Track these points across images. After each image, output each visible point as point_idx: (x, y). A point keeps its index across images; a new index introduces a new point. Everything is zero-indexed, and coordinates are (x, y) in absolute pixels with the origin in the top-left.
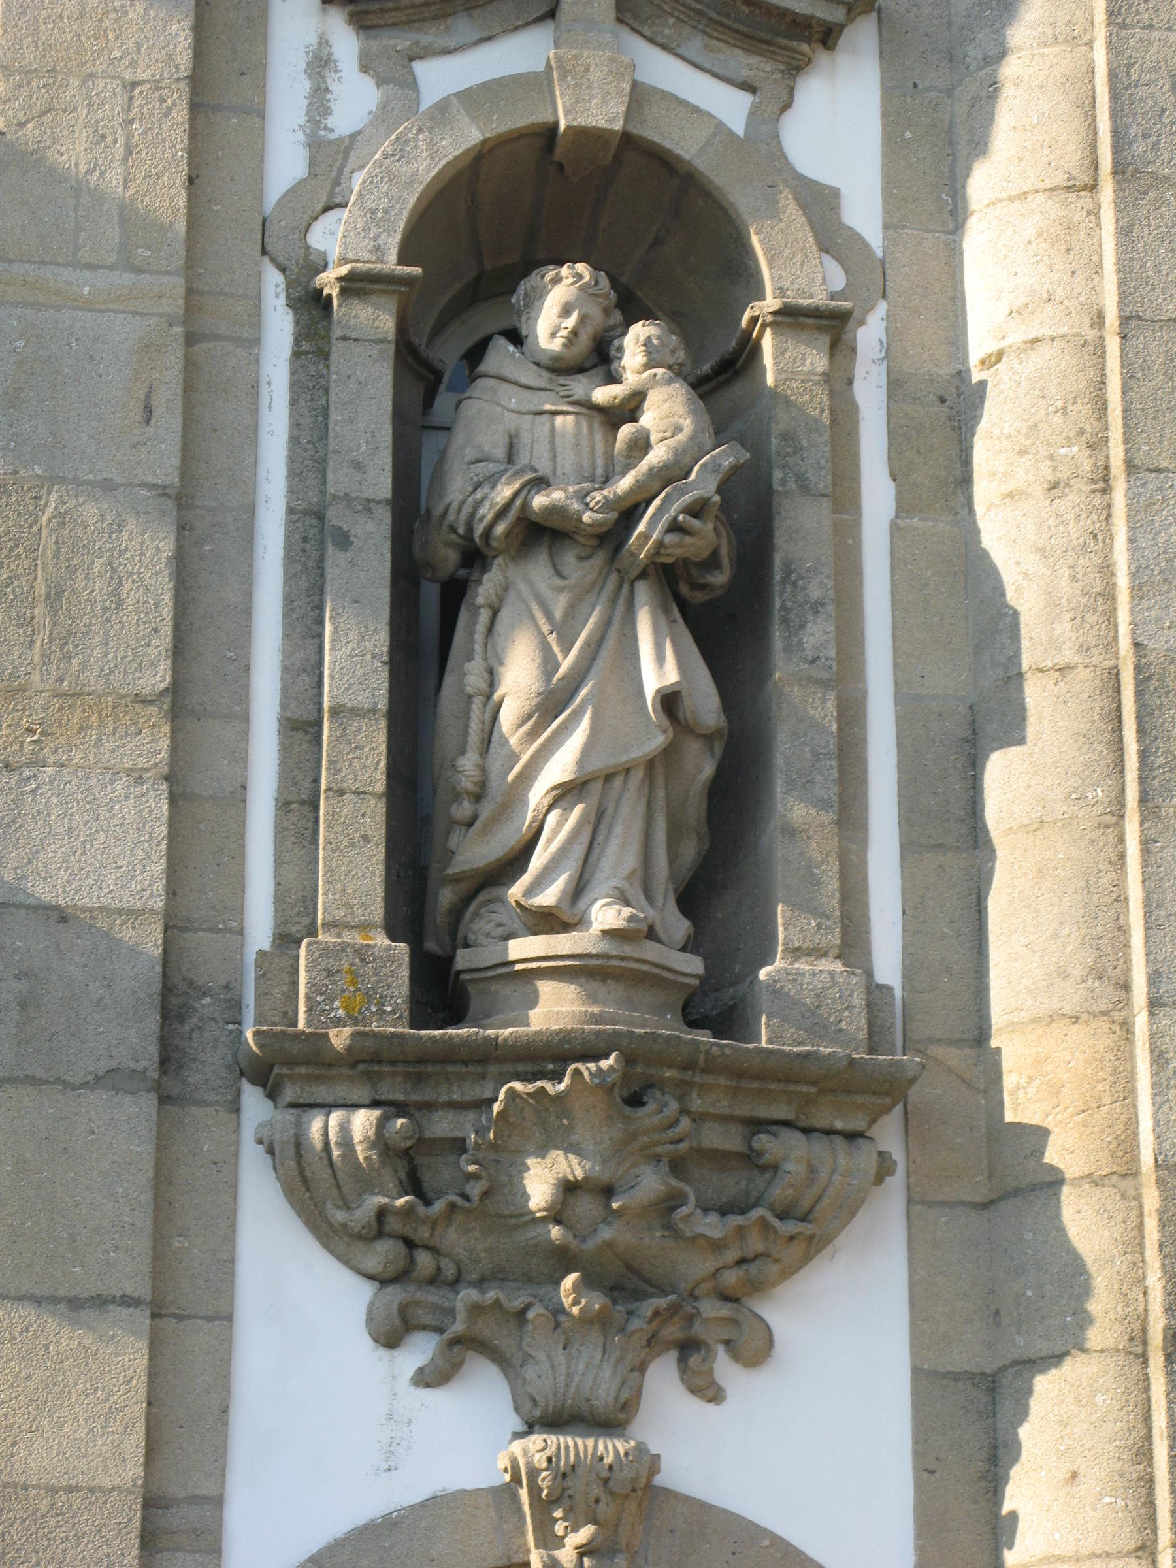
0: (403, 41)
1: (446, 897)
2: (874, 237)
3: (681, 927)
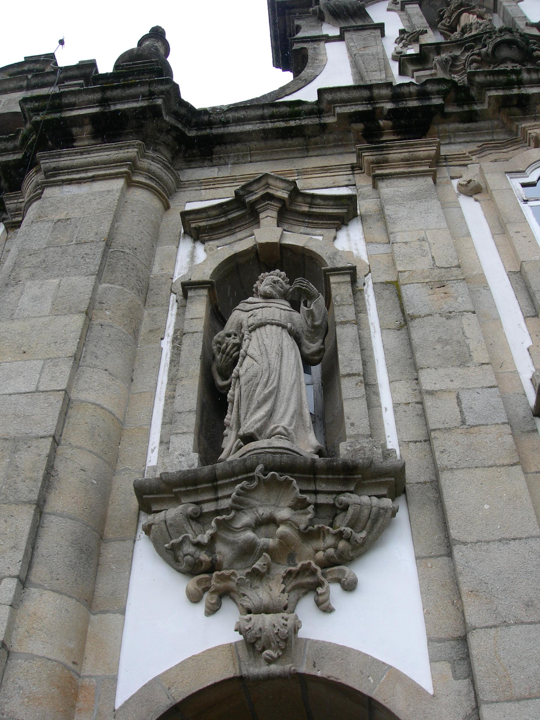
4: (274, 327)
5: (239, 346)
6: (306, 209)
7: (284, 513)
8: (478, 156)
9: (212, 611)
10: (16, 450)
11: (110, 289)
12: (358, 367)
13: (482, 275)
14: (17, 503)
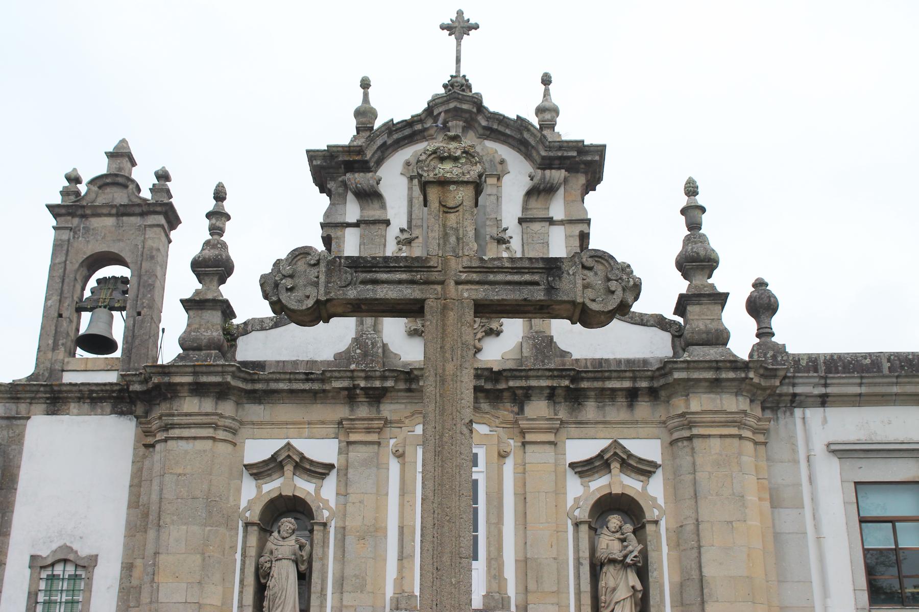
0: (587, 479)
2: (663, 505)
4: (286, 560)
5: (270, 568)
6: (308, 467)
8: (410, 419)
11: (210, 531)
12: (319, 587)
13: (386, 528)
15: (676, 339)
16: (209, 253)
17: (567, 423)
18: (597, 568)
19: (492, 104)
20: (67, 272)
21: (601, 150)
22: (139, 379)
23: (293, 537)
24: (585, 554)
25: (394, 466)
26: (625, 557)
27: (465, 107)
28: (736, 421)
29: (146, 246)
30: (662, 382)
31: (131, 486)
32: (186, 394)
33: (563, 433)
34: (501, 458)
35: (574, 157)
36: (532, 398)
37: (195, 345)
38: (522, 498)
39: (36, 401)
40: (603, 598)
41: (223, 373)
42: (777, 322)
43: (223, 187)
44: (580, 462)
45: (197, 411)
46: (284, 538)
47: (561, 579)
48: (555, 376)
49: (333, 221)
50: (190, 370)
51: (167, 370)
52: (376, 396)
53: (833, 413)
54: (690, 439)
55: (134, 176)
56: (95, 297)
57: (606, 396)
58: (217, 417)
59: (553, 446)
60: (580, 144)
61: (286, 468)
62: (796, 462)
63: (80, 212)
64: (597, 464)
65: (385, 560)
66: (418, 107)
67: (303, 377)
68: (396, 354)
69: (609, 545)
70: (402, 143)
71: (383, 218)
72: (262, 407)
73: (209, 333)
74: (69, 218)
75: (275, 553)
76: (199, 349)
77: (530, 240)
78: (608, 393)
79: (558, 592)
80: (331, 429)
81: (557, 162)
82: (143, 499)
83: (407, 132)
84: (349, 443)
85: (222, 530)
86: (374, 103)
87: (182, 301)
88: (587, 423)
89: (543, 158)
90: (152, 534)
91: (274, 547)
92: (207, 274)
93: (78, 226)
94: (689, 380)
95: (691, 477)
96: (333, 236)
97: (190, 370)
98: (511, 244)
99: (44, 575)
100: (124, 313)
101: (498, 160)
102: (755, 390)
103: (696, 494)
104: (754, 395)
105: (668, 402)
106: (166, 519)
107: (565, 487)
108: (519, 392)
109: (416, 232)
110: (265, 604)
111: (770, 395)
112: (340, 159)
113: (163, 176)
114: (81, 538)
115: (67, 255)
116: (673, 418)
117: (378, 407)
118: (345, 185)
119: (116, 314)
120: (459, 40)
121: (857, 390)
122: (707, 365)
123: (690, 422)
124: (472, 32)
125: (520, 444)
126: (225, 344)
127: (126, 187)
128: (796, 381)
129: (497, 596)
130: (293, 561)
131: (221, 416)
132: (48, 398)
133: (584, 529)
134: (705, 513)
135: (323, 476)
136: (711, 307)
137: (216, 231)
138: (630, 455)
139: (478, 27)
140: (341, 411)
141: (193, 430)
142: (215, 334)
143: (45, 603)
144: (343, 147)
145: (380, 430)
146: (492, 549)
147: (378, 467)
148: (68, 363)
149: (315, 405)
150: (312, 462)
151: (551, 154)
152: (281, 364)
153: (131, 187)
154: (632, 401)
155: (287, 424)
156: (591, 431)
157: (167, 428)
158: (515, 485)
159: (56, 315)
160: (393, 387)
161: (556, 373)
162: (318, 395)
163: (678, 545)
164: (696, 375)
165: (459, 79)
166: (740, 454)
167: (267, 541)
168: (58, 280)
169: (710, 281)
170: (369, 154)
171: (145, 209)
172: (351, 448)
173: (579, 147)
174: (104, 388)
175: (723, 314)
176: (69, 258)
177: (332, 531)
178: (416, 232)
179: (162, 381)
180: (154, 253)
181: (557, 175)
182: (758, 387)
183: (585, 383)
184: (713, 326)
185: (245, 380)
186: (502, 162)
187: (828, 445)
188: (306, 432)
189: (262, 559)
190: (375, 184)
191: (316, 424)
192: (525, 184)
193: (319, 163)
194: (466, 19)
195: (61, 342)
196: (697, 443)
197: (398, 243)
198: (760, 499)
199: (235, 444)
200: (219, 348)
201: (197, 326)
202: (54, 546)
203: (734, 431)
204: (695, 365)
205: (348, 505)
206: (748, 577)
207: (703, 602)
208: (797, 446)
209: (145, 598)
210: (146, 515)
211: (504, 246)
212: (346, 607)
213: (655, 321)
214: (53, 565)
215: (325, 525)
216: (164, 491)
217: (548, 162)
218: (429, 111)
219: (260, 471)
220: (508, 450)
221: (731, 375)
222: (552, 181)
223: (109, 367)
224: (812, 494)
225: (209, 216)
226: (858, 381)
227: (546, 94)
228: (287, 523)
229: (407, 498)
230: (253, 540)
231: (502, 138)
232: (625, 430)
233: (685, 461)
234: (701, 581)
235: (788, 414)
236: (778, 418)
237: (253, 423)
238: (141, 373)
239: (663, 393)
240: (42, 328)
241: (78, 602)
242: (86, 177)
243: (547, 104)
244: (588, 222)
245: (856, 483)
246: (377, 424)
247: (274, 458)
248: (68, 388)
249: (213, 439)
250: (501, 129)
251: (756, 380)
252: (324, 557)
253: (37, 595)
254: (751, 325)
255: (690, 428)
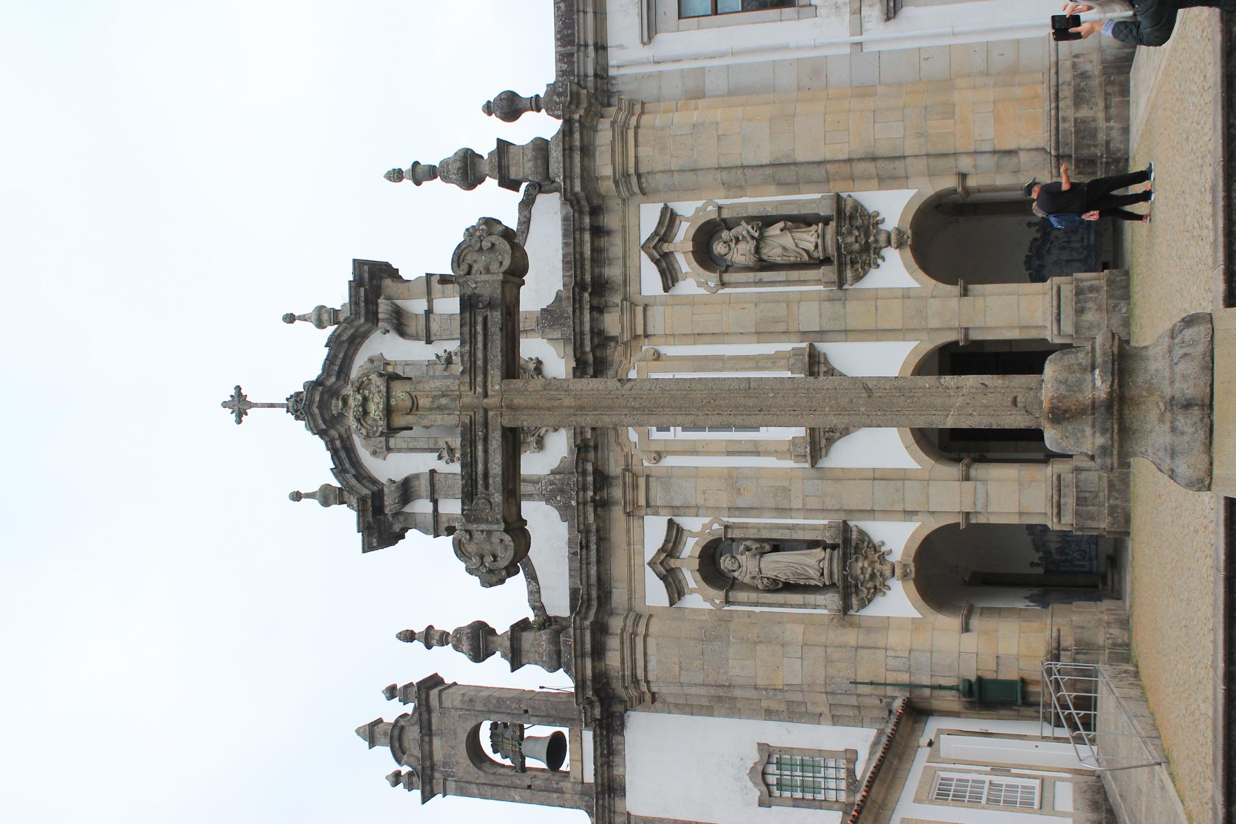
0: (679, 275)
1: (812, 261)
3: (814, 227)
5: (768, 578)
6: (671, 544)
7: (860, 564)
9: (890, 589)
10: (832, 661)
11: (734, 637)
13: (729, 468)
14: (856, 655)
15: (543, 190)
16: (466, 645)
17: (625, 294)
18: (764, 265)
19: (314, 371)
20: (487, 782)
21: (358, 264)
22: (589, 710)
23: (739, 557)
24: (751, 276)
25: (669, 461)
26: (753, 238)
27: (317, 398)
28: (621, 131)
29: (460, 707)
30: (584, 203)
31: (692, 714)
32: (603, 664)
33: (635, 298)
34: (661, 358)
35: (365, 289)
36: (602, 328)
37: (555, 656)
38: (698, 337)
39: (612, 807)
40: (792, 259)
41: (582, 629)
42: (525, 92)
43: (400, 633)
44: (663, 281)
45: (619, 653)
46: (740, 566)
47: (775, 299)
48: (580, 306)
49: (432, 526)
50: (579, 661)
51: (580, 683)
52: (602, 480)
53: (612, 40)
54: (639, 176)
55: (392, 721)
56: (511, 754)
57: (599, 256)
58: (625, 634)
59: (648, 308)
60: (353, 284)
61: (673, 566)
62: (660, 74)
63: (429, 772)
64: (664, 265)
65: (759, 468)
66: (318, 443)
67: (584, 552)
68: (561, 462)
69: (742, 253)
70: (354, 459)
71: (428, 477)
72: (614, 590)
73: (543, 643)
74: (434, 781)
75: (754, 574)
76: (559, 653)
77: (448, 332)
78: (595, 254)
79: (788, 302)
80: (635, 523)
81: (371, 307)
82: (704, 702)
83: (343, 454)
84: (648, 505)
85: (732, 626)
86: (315, 488)
87: (513, 670)
88: (625, 275)
89: (367, 320)
90: (737, 693)
91: (748, 576)
92: (486, 647)
93: (442, 772)
94: (582, 177)
95: (676, 174)
96: (447, 525)
97: (579, 661)
98: (452, 350)
99: (777, 793)
100: (526, 726)
101: (369, 365)
102: (592, 113)
103: (692, 170)
104: (596, 114)
105: (603, 197)
106: (722, 679)
107: (687, 296)
108: (596, 341)
109: (442, 444)
110: (802, 582)
111: (596, 99)
112: (371, 519)
113: (391, 692)
114: (742, 759)
115: (470, 783)
116: (619, 192)
117: (612, 478)
118: (397, 514)
119: (527, 734)
120: (252, 405)
121: (590, 16)
122: (568, 160)
123: (623, 175)
124: (244, 392)
125: (646, 340)
126: (554, 627)
127: (402, 728)
128: (582, 73)
129: (792, 361)
130: (761, 557)
131: (623, 630)
132: (609, 796)
133: (727, 277)
134: (711, 162)
135: (680, 530)
136: (511, 156)
137: (444, 639)
138: (656, 233)
139: (239, 386)
140: (617, 513)
141: (638, 656)
142: (544, 638)
143: (803, 792)
144: (359, 517)
145: (635, 476)
146: (747, 365)
147: (671, 477)
148: (575, 778)
149: (612, 539)
150: (667, 541)
151: (363, 312)
152: (573, 573)
153: (403, 723)
154: (603, 232)
155: (630, 566)
156: (632, 272)
157: (636, 681)
158: (686, 344)
159: (529, 791)
160: (593, 464)
161: (577, 306)
162: (602, 536)
163: (741, 187)
164: (578, 170)
165: (290, 405)
166: (653, 127)
167: (742, 582)
168: (495, 790)
169: (486, 157)
170: (365, 492)
171: (424, 709)
172: (652, 504)
173: (355, 285)
174: (598, 743)
175: (518, 144)
176: (473, 780)
177: (732, 520)
178: (442, 444)
179: (590, 688)
180: (466, 698)
181: (383, 307)
182: (588, 110)
183: (586, 277)
184: (530, 154)
185: (588, 608)
186: (371, 360)
187: (644, 43)
188: (638, 547)
189: (760, 587)
190: (395, 485)
191: (629, 537)
192: (393, 337)
193: (375, 540)
194: (230, 399)
195: (555, 786)
196: (642, 170)
197: (452, 461)
198: (696, 109)
199: (651, 616)
200: (557, 634)
201: (537, 656)
202: (750, 784)
203: (631, 133)
204: (568, 170)
205: (707, 505)
206: (770, 121)
207: (795, 164)
208: (645, 73)
209: (798, 697)
210: (719, 699)
211: (454, 358)
212: (804, 505)
213: (525, 210)
214: (767, 785)
215: (726, 527)
216: (696, 682)
217: (370, 316)
218: (321, 433)
219: (676, 590)
220: (653, 351)
221: (577, 136)
222: (389, 312)
223: (579, 739)
224: (690, 59)
225: (429, 647)
226: (581, 14)
227: (303, 318)
228: (725, 563)
229: (699, 448)
230: (742, 596)
231: (348, 361)
232: (631, 237)
233: (660, 180)
234: (774, 165)
235: (614, 82)
236: (618, 91)
237: (630, 599)
238: (584, 708)
239: (595, 202)
240: (542, 804)
241: (802, 760)
242: (395, 767)
243: (314, 318)
244: (429, 276)
245: (679, 18)
246: (628, 479)
247: (663, 578)
248: (599, 777)
249: (646, 636)
250: (338, 362)
251: (582, 112)
252: (758, 527)
253: (796, 799)
254: (528, 117)
255: (629, 176)
